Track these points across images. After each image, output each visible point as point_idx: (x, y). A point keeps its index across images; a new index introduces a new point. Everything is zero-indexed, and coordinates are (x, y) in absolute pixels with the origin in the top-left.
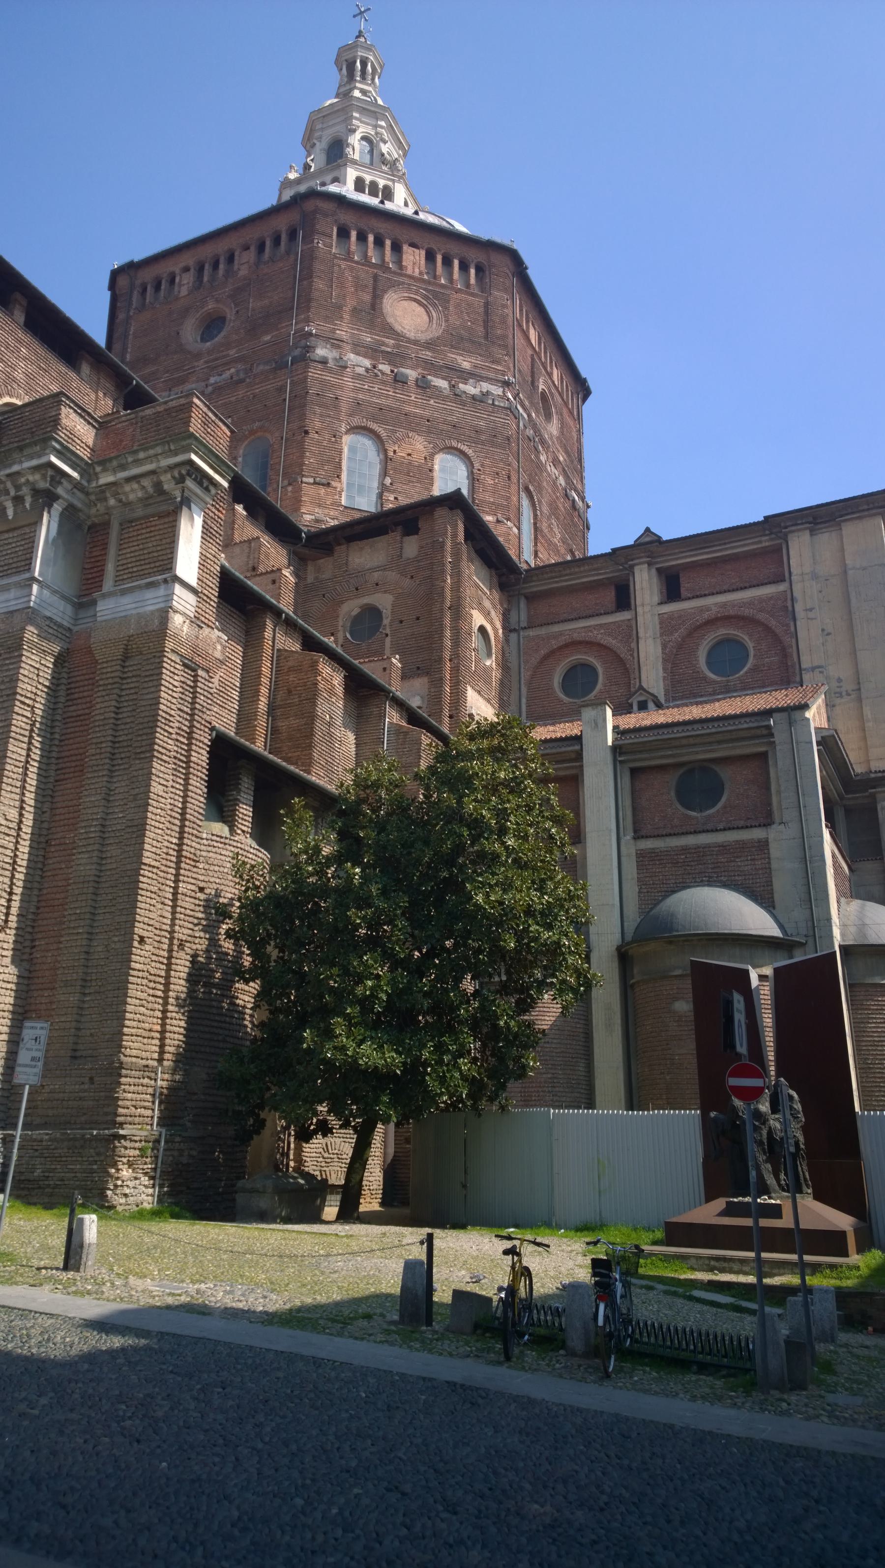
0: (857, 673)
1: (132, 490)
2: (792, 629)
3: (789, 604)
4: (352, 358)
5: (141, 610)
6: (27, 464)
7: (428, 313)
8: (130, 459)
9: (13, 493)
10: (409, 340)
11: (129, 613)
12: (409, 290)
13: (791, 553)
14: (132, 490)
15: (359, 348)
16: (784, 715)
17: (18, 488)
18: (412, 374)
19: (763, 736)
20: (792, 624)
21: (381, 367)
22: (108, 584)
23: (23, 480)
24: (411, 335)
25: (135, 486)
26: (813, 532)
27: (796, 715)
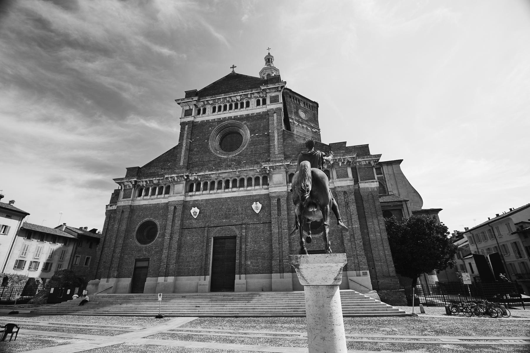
0: (399, 193)
1: (363, 163)
2: (385, 183)
3: (384, 179)
4: (296, 122)
5: (371, 186)
6: (349, 157)
7: (305, 114)
8: (365, 157)
9: (343, 161)
10: (303, 120)
11: (368, 187)
12: (302, 110)
13: (384, 169)
14: (363, 163)
15: (296, 120)
16: (404, 202)
17: (344, 160)
18: (305, 126)
19: (401, 206)
20: (385, 182)
21: (300, 124)
22: (359, 180)
23: (346, 159)
24: (303, 118)
25: (364, 162)
26: (387, 166)
27: (407, 202)
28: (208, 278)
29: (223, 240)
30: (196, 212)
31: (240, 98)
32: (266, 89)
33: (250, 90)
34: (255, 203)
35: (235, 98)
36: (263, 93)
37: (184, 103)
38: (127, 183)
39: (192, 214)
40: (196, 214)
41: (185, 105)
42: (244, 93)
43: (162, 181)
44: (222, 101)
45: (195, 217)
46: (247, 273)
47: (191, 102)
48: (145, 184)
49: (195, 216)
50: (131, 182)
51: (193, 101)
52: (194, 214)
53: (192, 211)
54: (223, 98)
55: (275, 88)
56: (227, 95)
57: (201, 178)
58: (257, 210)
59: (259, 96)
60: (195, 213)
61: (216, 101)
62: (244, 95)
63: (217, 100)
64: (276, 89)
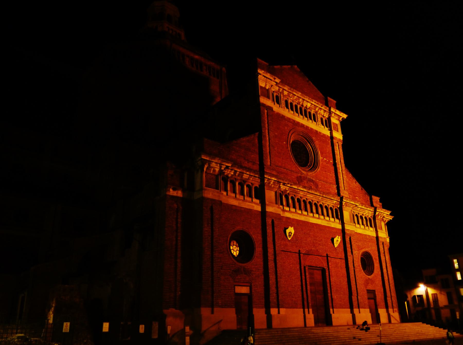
28: (311, 310)
29: (312, 271)
30: (291, 233)
31: (309, 106)
32: (333, 112)
33: (322, 104)
34: (337, 237)
35: (306, 104)
36: (327, 114)
37: (263, 77)
38: (215, 164)
39: (288, 234)
40: (291, 235)
41: (263, 80)
42: (315, 104)
43: (253, 178)
44: (295, 98)
45: (289, 239)
46: (338, 307)
47: (270, 81)
48: (232, 175)
49: (290, 237)
50: (221, 165)
51: (274, 81)
52: (289, 235)
53: (288, 231)
54: (298, 96)
55: (339, 116)
56: (303, 96)
57: (290, 191)
58: (336, 244)
59: (323, 114)
60: (290, 234)
61: (290, 95)
62: (315, 105)
63: (292, 95)
64: (339, 118)
